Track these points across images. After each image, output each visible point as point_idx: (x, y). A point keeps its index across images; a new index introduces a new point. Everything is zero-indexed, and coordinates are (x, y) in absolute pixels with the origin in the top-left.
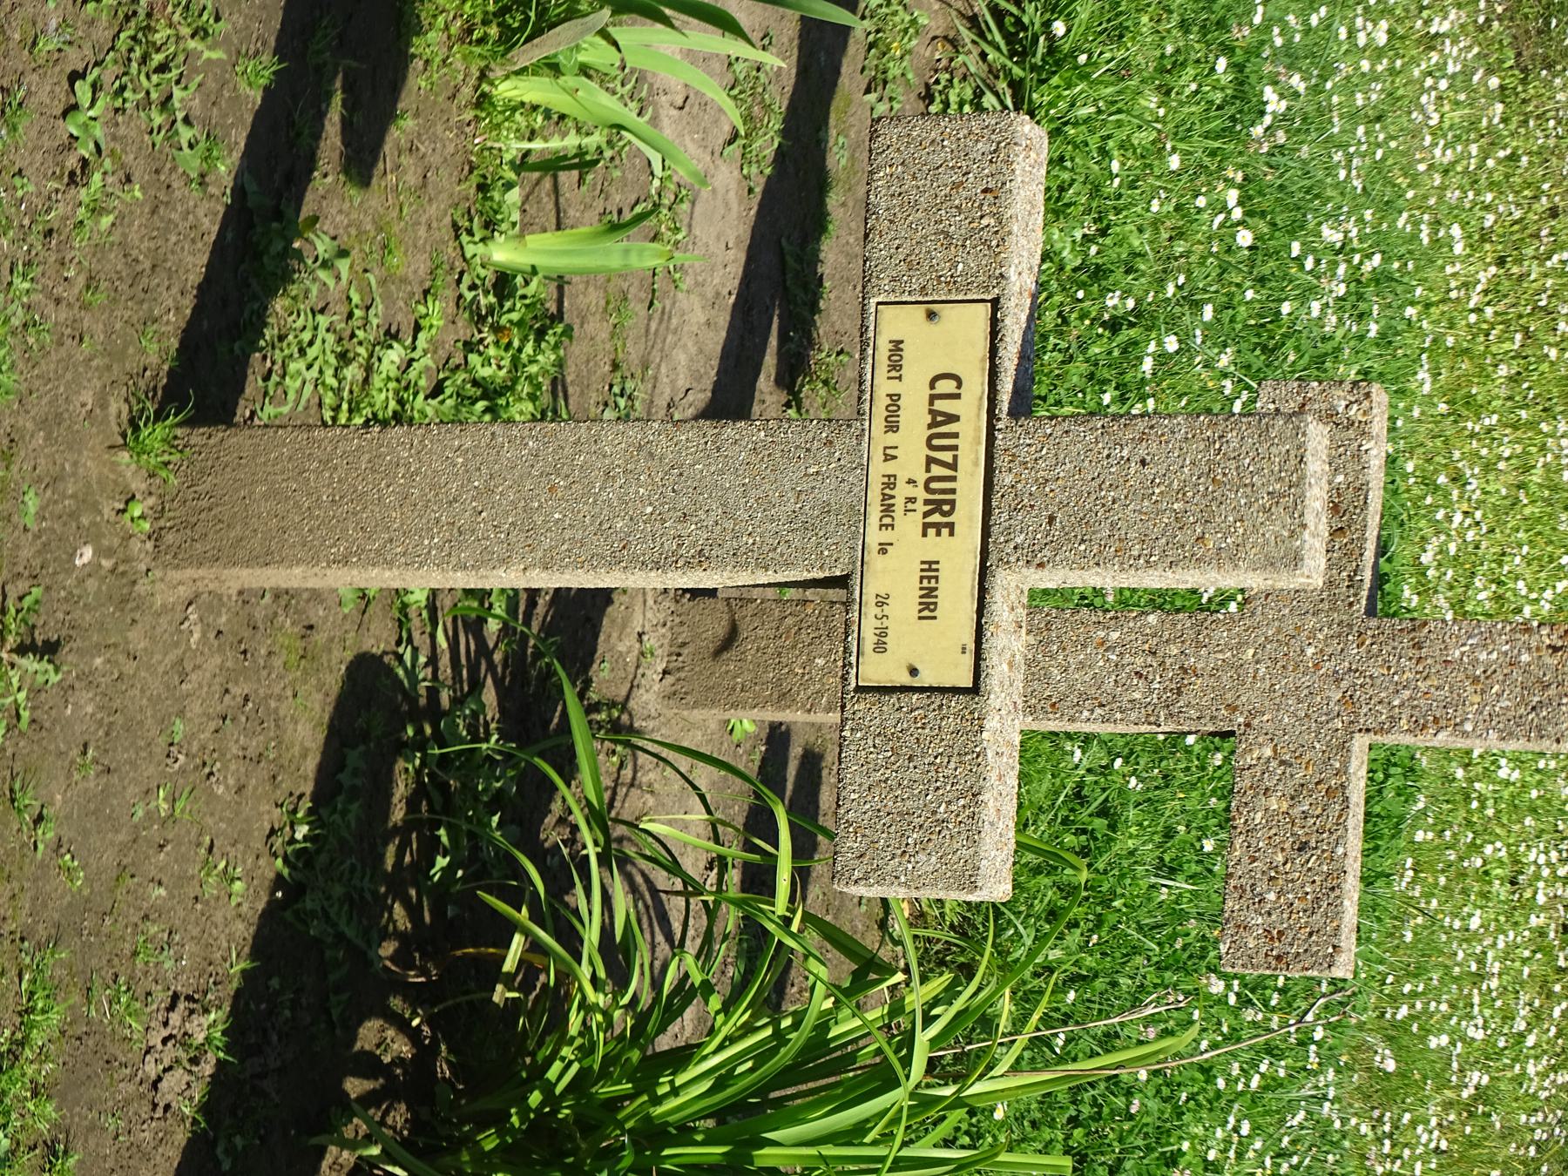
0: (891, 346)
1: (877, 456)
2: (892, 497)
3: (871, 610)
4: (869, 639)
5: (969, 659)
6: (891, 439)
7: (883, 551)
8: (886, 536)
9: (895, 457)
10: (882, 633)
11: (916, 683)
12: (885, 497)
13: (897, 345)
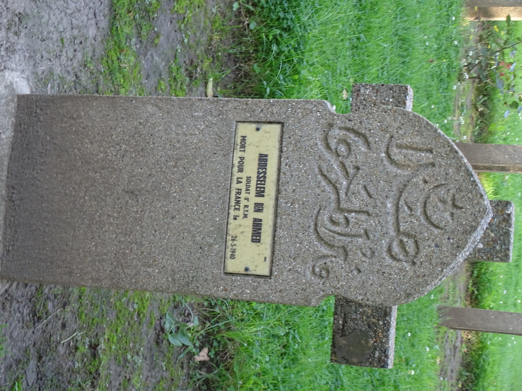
0: (241, 138)
1: (235, 181)
2: (240, 198)
6: (240, 175)
7: (235, 219)
8: (237, 213)
9: (241, 182)
12: (237, 198)
13: (244, 138)
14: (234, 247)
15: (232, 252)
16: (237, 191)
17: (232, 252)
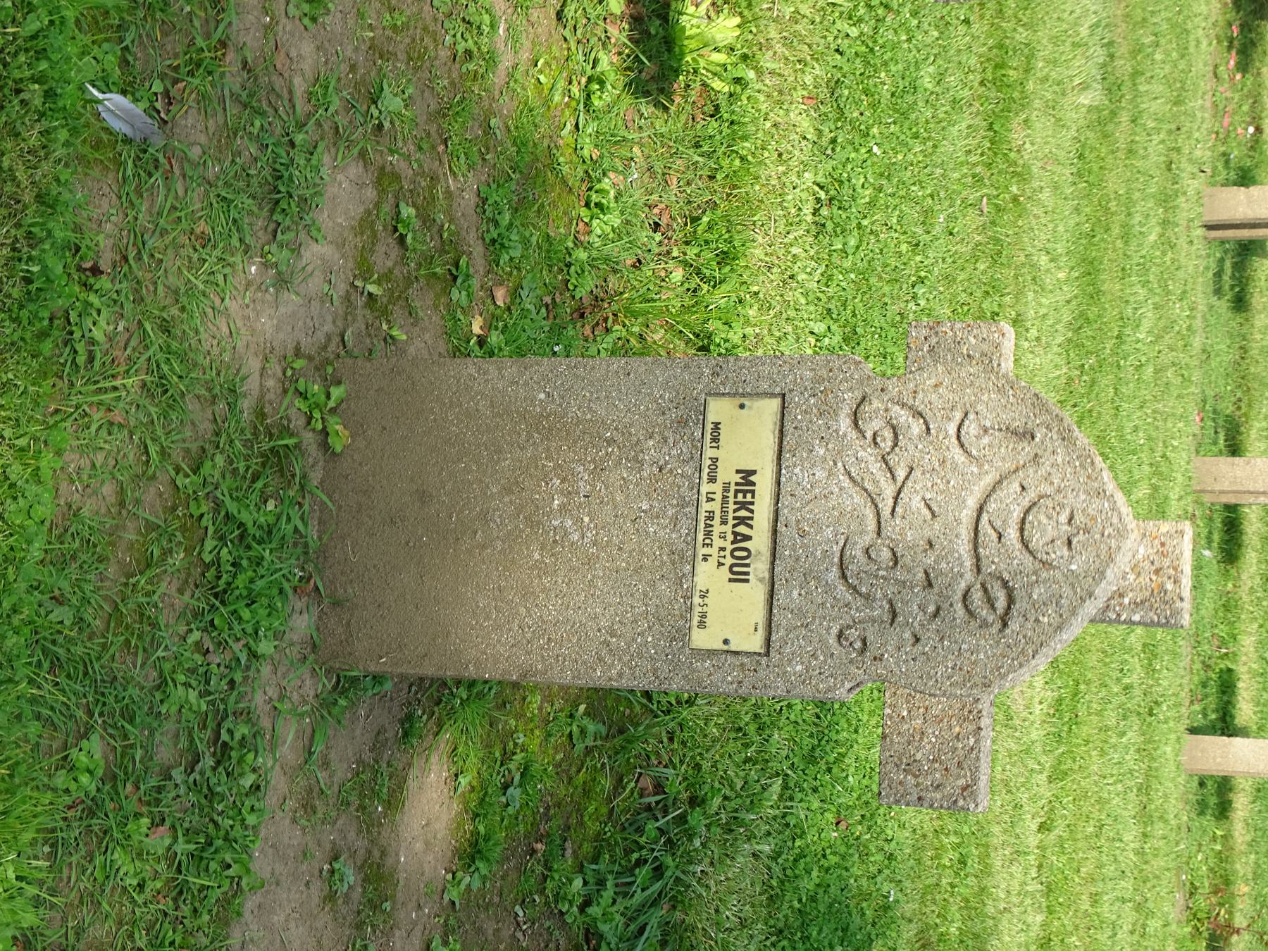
0: (712, 426)
2: (712, 526)
3: (697, 600)
4: (696, 620)
5: (761, 633)
7: (705, 560)
8: (706, 551)
9: (713, 500)
11: (726, 648)
15: (701, 617)
16: (707, 514)
17: (701, 617)
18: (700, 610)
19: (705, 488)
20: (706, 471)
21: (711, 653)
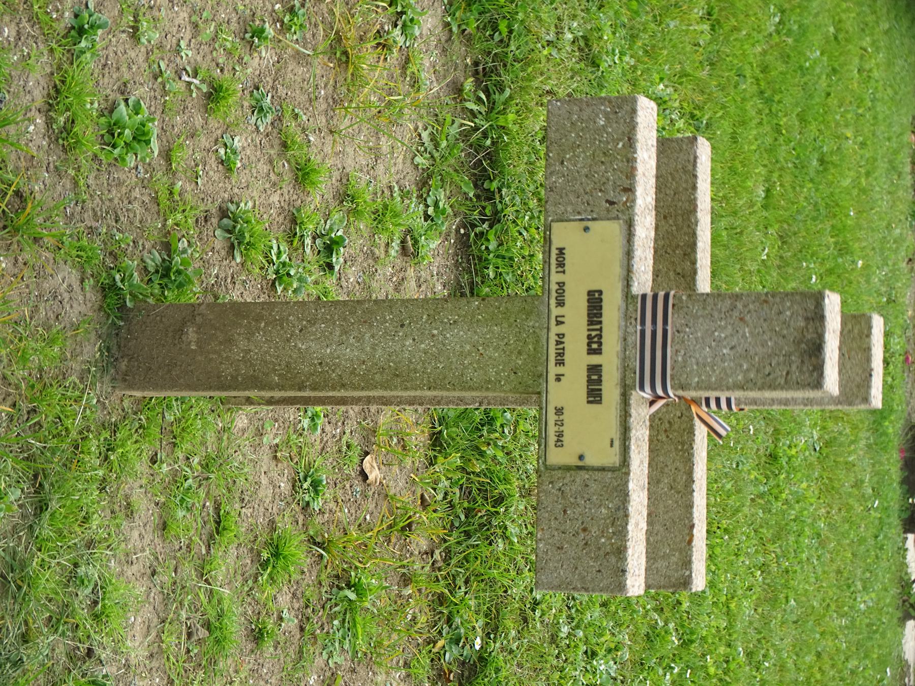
3: (552, 418)
4: (552, 439)
9: (563, 323)
10: (560, 435)
14: (562, 429)
18: (556, 428)
19: (555, 311)
20: (554, 295)
21: (568, 468)
